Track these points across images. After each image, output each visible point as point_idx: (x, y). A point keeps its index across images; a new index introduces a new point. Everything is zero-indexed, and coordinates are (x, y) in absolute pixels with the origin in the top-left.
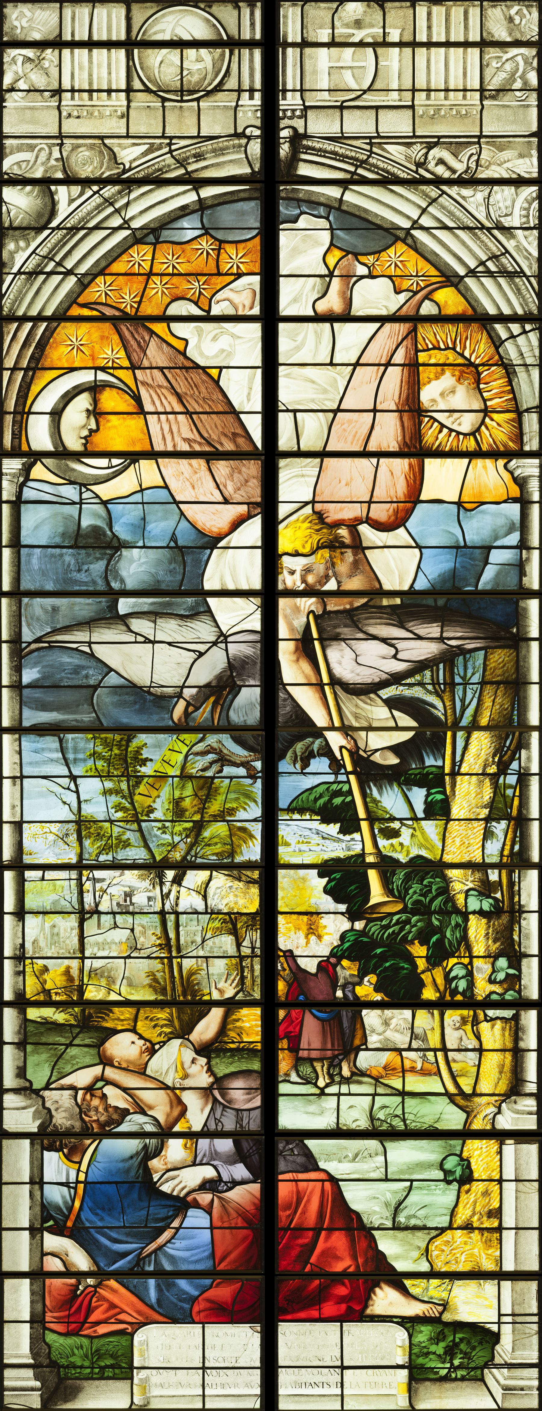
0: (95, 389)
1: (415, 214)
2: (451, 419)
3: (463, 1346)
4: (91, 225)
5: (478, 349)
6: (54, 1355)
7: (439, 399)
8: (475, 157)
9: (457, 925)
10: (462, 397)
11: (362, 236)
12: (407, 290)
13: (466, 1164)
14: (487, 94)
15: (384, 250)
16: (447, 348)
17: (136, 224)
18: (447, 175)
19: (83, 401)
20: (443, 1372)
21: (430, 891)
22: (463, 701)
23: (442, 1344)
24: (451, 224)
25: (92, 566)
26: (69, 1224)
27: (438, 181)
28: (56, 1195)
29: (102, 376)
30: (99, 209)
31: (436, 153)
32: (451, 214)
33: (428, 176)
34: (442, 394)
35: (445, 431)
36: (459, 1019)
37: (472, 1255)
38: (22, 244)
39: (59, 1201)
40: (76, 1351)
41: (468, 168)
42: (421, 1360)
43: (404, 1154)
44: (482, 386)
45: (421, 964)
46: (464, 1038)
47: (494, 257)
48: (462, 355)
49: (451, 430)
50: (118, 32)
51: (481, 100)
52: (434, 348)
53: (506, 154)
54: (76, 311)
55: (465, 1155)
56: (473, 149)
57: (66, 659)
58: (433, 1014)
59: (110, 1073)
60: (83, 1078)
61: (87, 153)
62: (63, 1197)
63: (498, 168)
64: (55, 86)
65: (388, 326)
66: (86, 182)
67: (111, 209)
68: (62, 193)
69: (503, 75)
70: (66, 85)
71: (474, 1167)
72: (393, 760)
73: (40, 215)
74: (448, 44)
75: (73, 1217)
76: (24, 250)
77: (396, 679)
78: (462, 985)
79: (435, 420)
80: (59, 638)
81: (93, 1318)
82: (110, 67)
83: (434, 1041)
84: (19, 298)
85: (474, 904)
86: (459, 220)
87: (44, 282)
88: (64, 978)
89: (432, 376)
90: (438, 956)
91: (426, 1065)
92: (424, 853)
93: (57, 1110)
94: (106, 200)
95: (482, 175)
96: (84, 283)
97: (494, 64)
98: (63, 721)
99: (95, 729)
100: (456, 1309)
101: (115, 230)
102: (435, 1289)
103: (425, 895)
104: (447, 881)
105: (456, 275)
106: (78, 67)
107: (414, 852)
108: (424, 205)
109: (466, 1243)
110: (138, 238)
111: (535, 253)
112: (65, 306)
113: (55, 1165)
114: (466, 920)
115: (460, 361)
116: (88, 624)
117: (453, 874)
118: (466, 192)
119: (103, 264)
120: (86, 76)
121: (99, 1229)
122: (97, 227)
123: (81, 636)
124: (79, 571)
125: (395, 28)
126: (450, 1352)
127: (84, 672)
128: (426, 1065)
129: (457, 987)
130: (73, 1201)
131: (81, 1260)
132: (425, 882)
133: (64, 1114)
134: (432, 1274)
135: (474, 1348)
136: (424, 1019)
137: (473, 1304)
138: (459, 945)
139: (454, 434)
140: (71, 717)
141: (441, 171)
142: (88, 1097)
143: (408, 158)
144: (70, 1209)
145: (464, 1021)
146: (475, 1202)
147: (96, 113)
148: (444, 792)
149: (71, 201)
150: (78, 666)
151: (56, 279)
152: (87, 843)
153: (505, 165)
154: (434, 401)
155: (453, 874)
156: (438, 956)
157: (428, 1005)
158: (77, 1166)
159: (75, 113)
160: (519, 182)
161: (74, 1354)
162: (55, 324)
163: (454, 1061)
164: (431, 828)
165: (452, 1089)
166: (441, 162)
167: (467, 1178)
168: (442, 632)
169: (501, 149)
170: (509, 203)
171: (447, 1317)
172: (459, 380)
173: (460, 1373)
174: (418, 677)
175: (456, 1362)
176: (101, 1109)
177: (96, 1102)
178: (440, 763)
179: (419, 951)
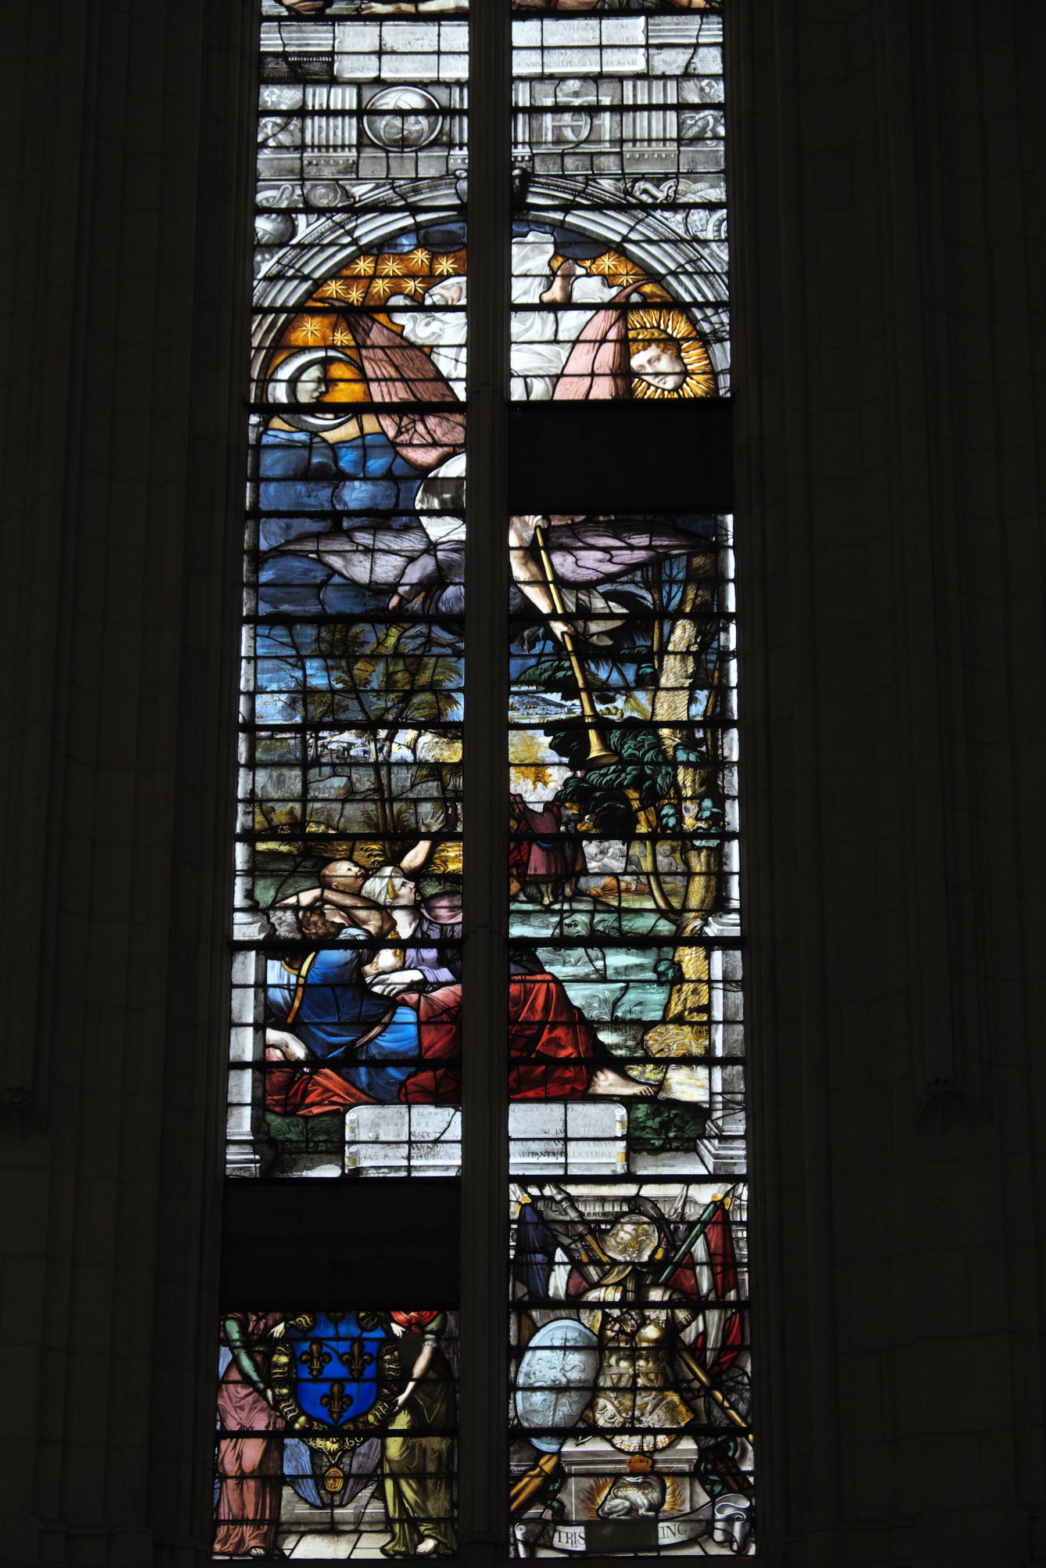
0: (325, 363)
1: (624, 231)
2: (657, 380)
3: (677, 1121)
4: (326, 241)
5: (679, 328)
6: (273, 1132)
7: (647, 365)
8: (674, 188)
9: (667, 773)
10: (665, 364)
11: (575, 247)
12: (620, 285)
13: (677, 966)
14: (683, 142)
15: (600, 257)
16: (653, 327)
17: (364, 241)
18: (650, 201)
19: (314, 372)
20: (657, 1143)
21: (643, 746)
22: (669, 593)
23: (658, 1120)
24: (655, 238)
25: (320, 493)
26: (289, 1020)
27: (643, 206)
28: (277, 996)
29: (332, 353)
30: (332, 230)
31: (641, 185)
32: (655, 230)
33: (634, 201)
34: (649, 362)
35: (652, 388)
36: (669, 848)
37: (683, 1044)
38: (267, 256)
39: (280, 1000)
40: (292, 1129)
41: (668, 196)
42: (637, 1134)
43: (618, 959)
44: (683, 354)
45: (636, 805)
46: (674, 864)
47: (690, 261)
48: (665, 331)
49: (657, 388)
50: (351, 104)
51: (678, 147)
52: (642, 327)
53: (699, 186)
54: (311, 304)
55: (676, 959)
56: (671, 183)
57: (297, 564)
58: (645, 845)
59: (329, 895)
60: (306, 898)
61: (323, 190)
62: (284, 998)
63: (693, 196)
64: (298, 142)
65: (602, 313)
66: (321, 212)
67: (342, 231)
68: (301, 220)
69: (696, 129)
70: (308, 140)
71: (684, 970)
72: (608, 642)
73: (282, 235)
74: (650, 108)
75: (292, 1015)
76: (268, 261)
77: (610, 578)
78: (672, 822)
79: (644, 381)
80: (291, 547)
81: (308, 1101)
82: (348, 130)
83: (647, 865)
84: (264, 295)
85: (682, 756)
86: (662, 234)
87: (285, 284)
88: (288, 817)
89: (640, 347)
90: (652, 798)
91: (640, 886)
92: (636, 715)
93: (280, 924)
94: (338, 224)
95: (682, 200)
96: (319, 283)
97: (689, 122)
98: (294, 611)
99: (319, 620)
100: (670, 1089)
101: (344, 246)
102: (651, 1073)
103: (639, 750)
104: (659, 739)
105: (659, 274)
106: (315, 129)
107: (627, 714)
108: (632, 224)
109: (677, 1034)
110: (364, 251)
111: (726, 258)
112: (303, 299)
113: (276, 972)
114: (675, 769)
115: (663, 336)
116: (317, 536)
117: (665, 732)
118: (667, 214)
119: (335, 270)
120: (324, 135)
121: (316, 1025)
122: (331, 244)
123: (310, 546)
124: (309, 496)
125: (606, 96)
126: (665, 1126)
127: (312, 574)
128: (640, 886)
129: (667, 823)
130: (293, 1001)
131: (298, 1050)
132: (639, 739)
133: (286, 928)
134: (647, 1059)
135: (687, 1123)
136: (636, 849)
137: (688, 1086)
138: (669, 789)
139: (659, 391)
140: (300, 608)
141: (644, 197)
142: (308, 914)
143: (618, 189)
144: (290, 1006)
145: (673, 850)
146: (686, 999)
147: (332, 162)
148: (653, 667)
149: (308, 225)
150: (308, 569)
151: (296, 282)
152: (311, 708)
153: (699, 194)
154: (642, 366)
155: (665, 732)
156: (652, 798)
157: (642, 838)
158: (296, 972)
159: (315, 162)
160: (711, 207)
161: (290, 1131)
162: (293, 315)
163: (666, 883)
164: (642, 697)
165: (662, 904)
166: (645, 191)
167: (679, 979)
168: (651, 541)
169: (695, 182)
170: (704, 222)
171: (662, 1095)
172: (663, 351)
173: (675, 1144)
174: (630, 576)
175: (672, 1135)
176: (319, 924)
177: (314, 918)
178: (649, 643)
179: (633, 794)
